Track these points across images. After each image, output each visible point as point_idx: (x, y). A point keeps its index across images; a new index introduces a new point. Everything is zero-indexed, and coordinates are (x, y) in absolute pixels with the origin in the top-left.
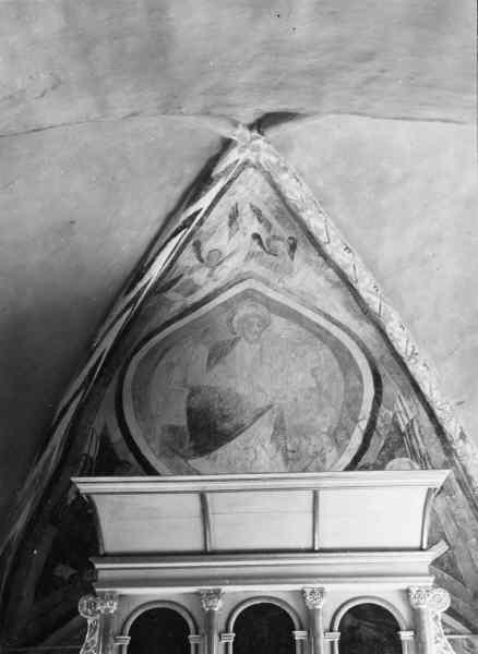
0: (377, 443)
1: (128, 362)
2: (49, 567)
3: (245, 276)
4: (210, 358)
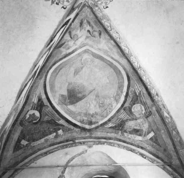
0: (129, 100)
2: (19, 141)
4: (74, 73)
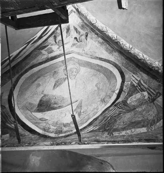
1: (22, 75)
3: (71, 52)
